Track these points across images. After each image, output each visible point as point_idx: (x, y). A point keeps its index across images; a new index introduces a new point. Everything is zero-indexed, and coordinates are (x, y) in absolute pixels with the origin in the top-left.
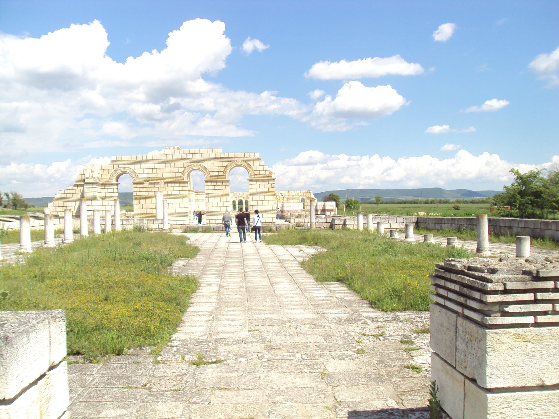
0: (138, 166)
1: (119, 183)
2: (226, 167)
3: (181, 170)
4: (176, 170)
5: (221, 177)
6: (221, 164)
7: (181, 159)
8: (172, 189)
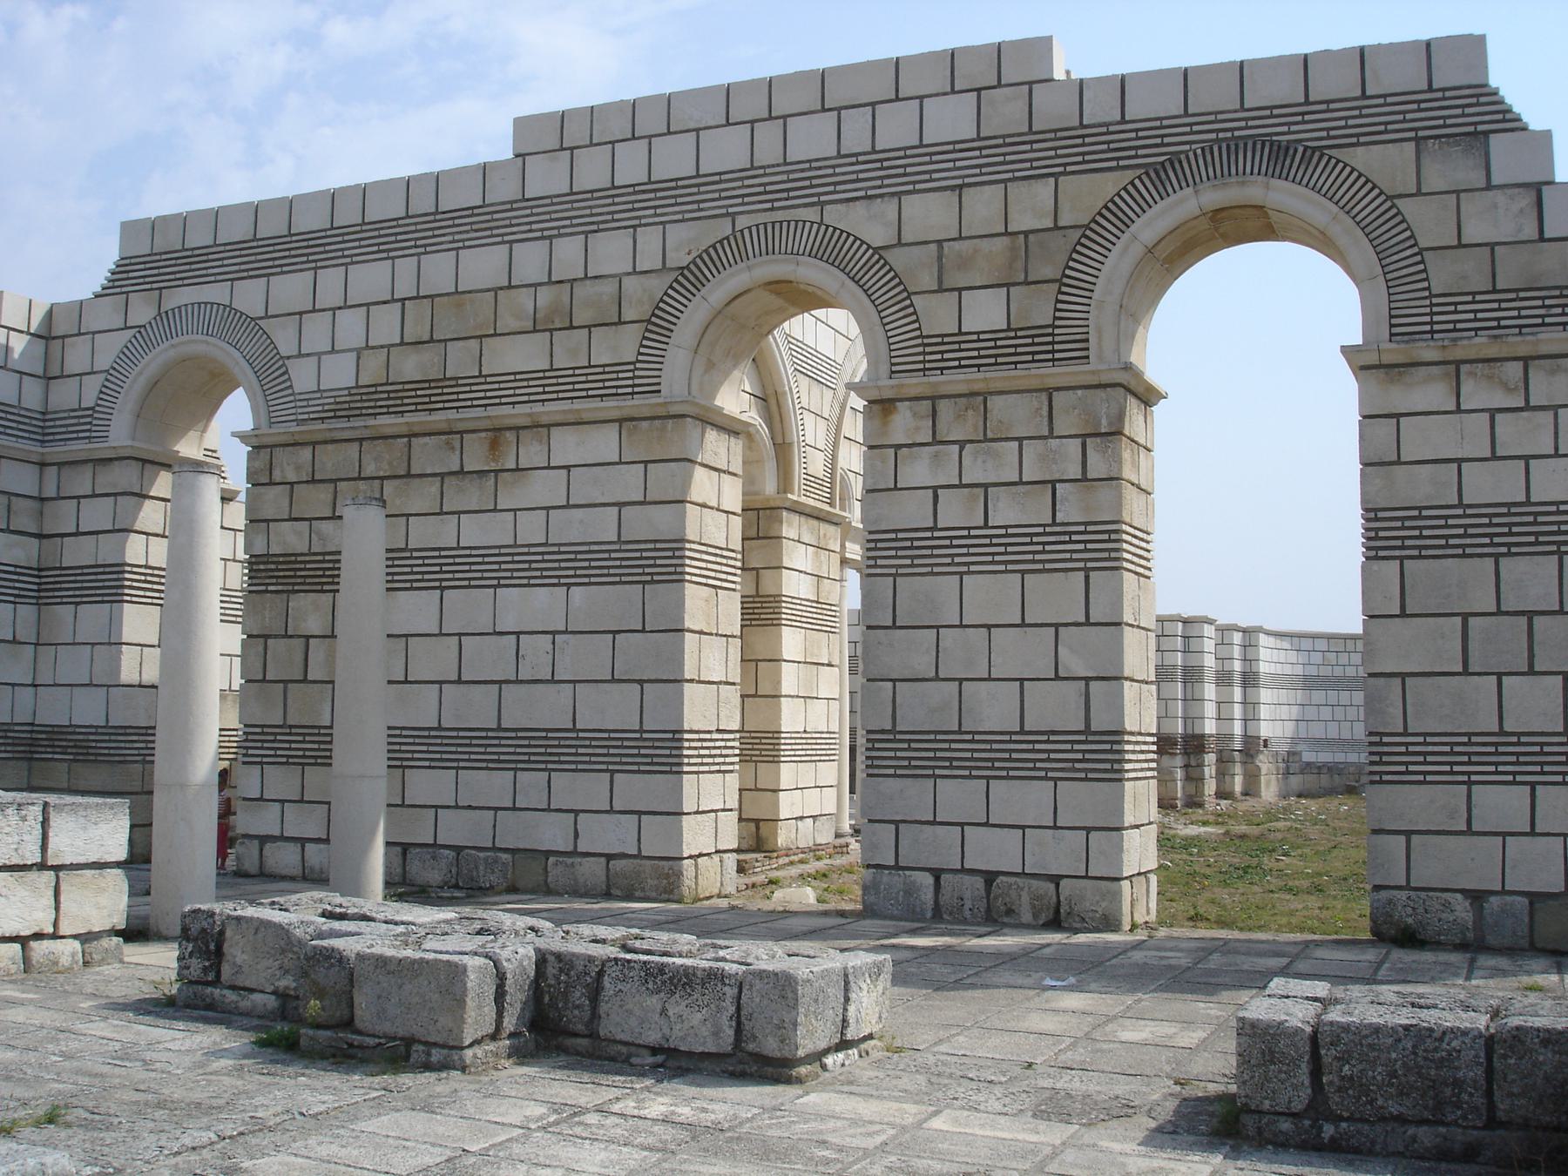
0: (291, 289)
3: (640, 295)
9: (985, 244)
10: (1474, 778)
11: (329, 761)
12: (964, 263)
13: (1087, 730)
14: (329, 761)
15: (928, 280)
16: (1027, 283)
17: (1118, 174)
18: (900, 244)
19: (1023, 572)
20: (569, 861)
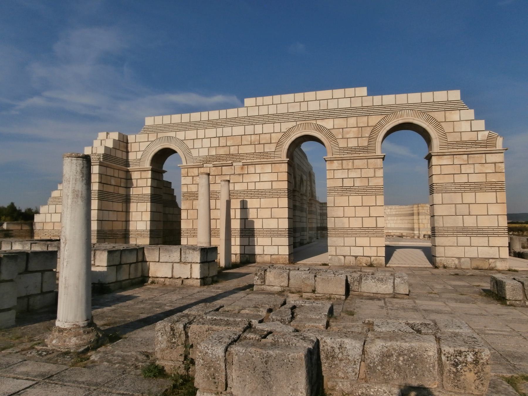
0: (191, 134)
1: (165, 172)
2: (375, 129)
3: (275, 138)
4: (265, 138)
5: (365, 149)
6: (363, 121)
7: (277, 115)
8: (256, 178)
9: (353, 129)
10: (458, 235)
11: (432, 230)
12: (348, 133)
13: (376, 227)
14: (432, 230)
15: (340, 137)
16: (362, 137)
17: (381, 116)
18: (334, 129)
19: (362, 195)
20: (262, 256)
